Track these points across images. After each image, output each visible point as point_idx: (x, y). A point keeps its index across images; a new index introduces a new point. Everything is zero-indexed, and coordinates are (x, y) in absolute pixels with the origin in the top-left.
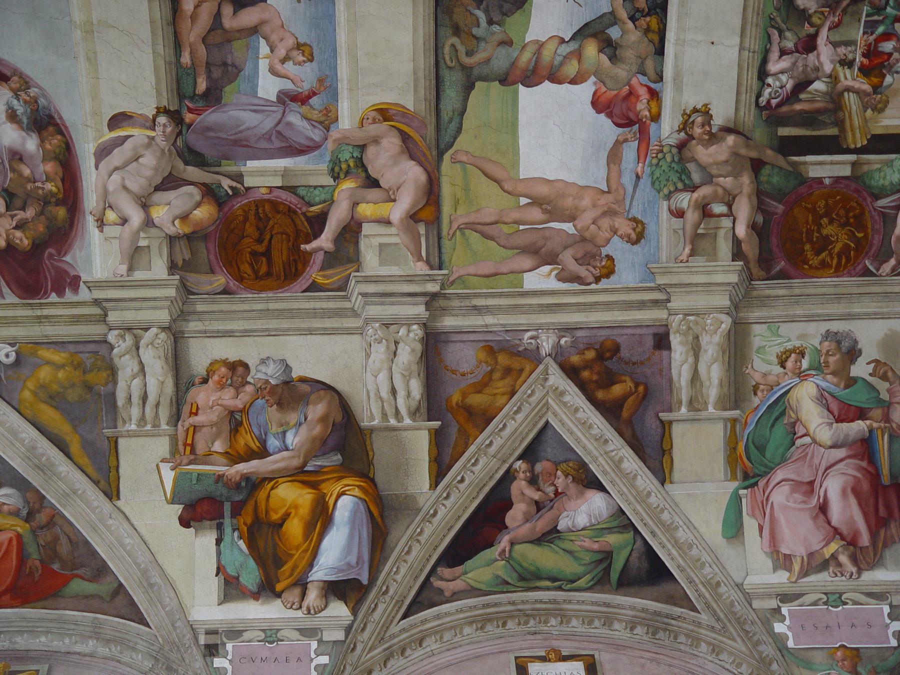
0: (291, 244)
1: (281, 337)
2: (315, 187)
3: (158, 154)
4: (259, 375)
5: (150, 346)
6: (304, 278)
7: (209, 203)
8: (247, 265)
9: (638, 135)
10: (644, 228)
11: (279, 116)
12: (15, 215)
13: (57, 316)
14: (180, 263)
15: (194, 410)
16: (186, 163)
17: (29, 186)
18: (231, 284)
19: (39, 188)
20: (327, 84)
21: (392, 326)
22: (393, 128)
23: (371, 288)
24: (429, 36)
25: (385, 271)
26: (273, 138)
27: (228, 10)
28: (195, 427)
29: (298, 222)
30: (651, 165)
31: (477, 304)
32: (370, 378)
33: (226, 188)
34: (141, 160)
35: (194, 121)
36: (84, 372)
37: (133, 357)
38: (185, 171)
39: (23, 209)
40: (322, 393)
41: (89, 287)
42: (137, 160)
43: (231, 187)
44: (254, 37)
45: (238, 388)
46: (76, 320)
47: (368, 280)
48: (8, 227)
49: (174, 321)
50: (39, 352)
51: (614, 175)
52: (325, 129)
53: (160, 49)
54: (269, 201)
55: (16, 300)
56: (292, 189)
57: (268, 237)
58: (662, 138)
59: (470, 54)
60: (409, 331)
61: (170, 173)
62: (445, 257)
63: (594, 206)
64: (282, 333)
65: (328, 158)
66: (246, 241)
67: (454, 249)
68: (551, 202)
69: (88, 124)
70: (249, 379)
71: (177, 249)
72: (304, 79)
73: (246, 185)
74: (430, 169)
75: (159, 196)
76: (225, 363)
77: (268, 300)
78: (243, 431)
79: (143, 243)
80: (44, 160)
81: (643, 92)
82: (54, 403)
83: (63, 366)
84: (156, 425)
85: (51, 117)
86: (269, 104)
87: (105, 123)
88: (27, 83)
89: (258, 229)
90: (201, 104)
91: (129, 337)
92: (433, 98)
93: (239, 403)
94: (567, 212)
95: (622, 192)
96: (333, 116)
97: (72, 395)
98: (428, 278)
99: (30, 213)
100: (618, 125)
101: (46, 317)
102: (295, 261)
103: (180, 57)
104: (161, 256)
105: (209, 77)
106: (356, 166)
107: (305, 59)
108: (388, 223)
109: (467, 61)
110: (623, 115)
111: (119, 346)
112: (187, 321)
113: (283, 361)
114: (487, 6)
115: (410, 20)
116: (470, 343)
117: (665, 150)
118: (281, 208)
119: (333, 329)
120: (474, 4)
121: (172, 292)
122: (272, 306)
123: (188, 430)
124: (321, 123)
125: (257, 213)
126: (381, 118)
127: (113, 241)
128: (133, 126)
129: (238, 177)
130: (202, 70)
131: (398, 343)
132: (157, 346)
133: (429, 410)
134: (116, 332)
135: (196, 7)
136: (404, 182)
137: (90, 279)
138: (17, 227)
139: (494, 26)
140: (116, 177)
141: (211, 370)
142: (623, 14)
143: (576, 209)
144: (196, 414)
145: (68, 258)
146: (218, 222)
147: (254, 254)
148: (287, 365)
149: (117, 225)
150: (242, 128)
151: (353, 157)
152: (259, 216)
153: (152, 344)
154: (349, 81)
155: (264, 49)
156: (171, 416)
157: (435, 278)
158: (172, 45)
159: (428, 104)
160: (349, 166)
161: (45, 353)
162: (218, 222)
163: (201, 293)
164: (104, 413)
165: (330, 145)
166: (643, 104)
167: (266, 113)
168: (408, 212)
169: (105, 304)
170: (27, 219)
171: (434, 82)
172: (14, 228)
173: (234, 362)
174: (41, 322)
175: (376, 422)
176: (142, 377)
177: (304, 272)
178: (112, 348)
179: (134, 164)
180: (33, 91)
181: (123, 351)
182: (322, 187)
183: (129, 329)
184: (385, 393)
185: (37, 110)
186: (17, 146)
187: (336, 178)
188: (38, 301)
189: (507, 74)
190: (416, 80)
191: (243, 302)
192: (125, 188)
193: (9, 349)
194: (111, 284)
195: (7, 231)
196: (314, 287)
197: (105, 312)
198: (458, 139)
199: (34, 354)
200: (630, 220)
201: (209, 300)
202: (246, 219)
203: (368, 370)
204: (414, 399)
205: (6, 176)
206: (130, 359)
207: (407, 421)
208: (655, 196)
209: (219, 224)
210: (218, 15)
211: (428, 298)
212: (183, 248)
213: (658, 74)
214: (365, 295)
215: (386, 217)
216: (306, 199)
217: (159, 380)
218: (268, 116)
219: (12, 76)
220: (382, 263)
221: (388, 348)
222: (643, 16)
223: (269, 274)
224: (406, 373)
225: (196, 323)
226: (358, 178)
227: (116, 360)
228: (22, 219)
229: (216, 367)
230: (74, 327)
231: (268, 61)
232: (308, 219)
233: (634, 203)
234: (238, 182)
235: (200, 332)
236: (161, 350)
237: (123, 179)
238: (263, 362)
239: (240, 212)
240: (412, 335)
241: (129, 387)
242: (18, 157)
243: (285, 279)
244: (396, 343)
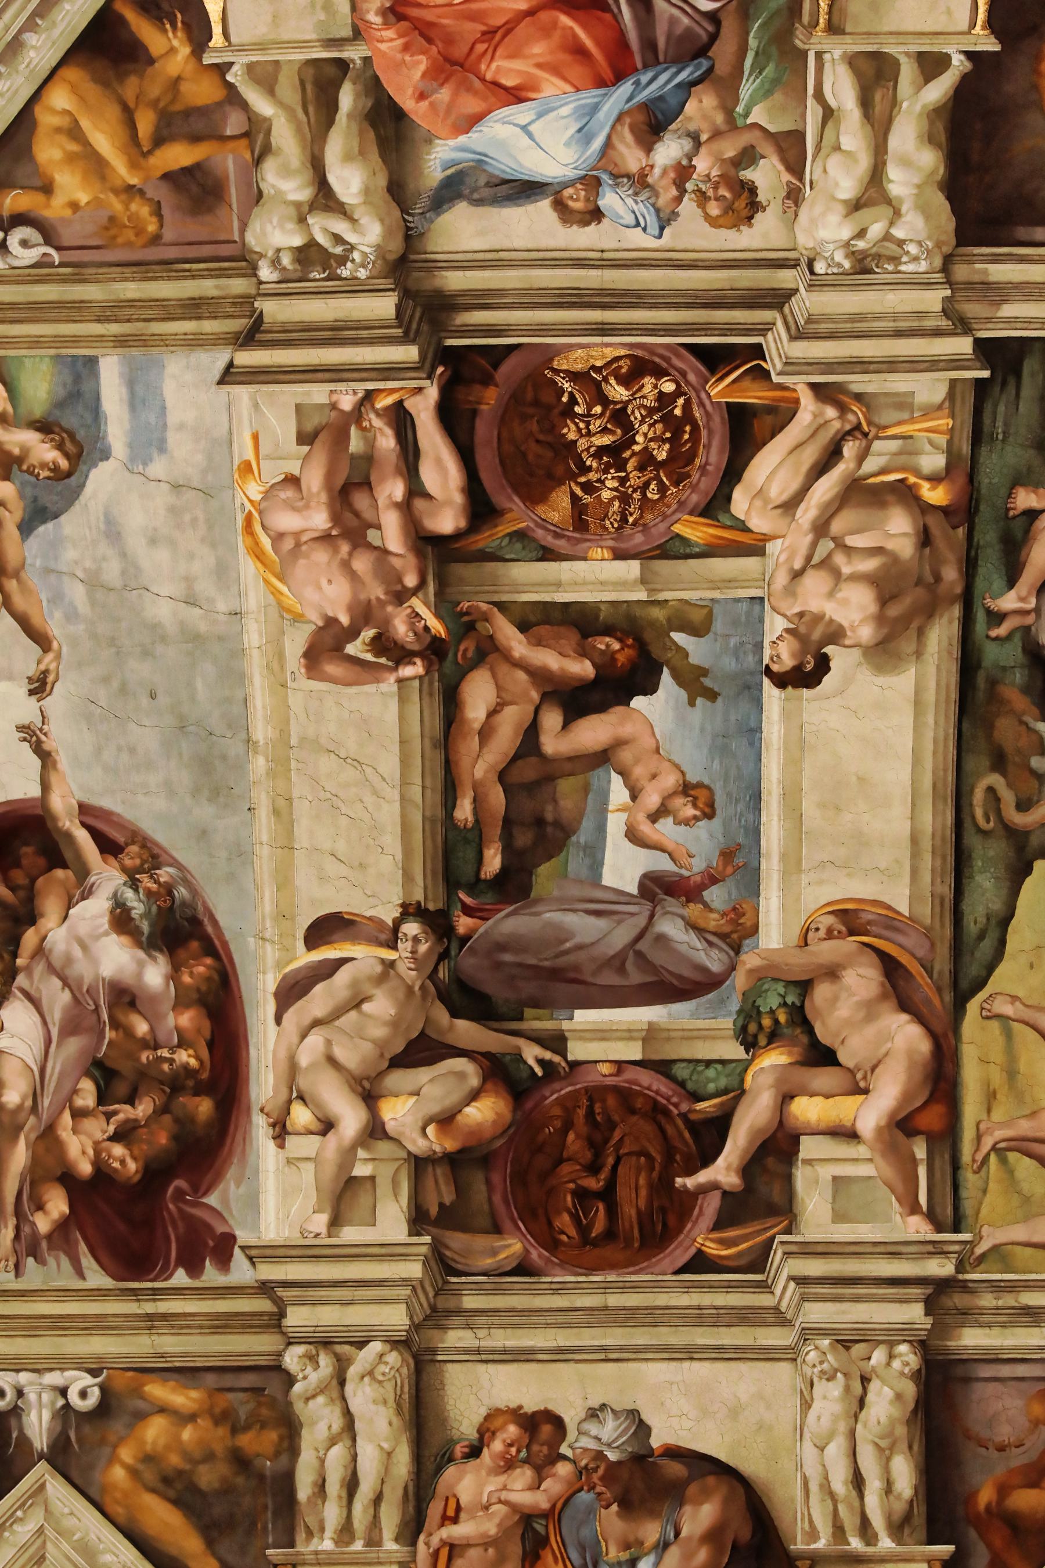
0: (655, 1174)
1: (631, 1365)
2: (708, 1063)
3: (401, 994)
4: (586, 1442)
5: (367, 1379)
6: (680, 1244)
7: (497, 1094)
8: (566, 1217)
11: (642, 921)
12: (115, 1113)
13: (185, 1315)
14: (434, 1210)
15: (451, 1512)
16: (455, 1014)
17: (145, 1056)
18: (534, 1255)
19: (162, 1059)
20: (739, 860)
21: (857, 1345)
22: (868, 950)
23: (814, 1267)
25: (844, 1233)
26: (630, 966)
27: (552, 719)
28: (452, 1547)
29: (670, 1130)
31: (1031, 1303)
32: (809, 1452)
33: (531, 1062)
34: (366, 1007)
35: (474, 930)
36: (235, 1431)
37: (332, 1400)
38: (451, 1027)
39: (131, 1101)
40: (711, 1480)
41: (251, 1259)
42: (358, 1005)
43: (541, 1062)
44: (600, 772)
45: (542, 1468)
46: (223, 1323)
47: (809, 1250)
48: (99, 1136)
49: (416, 1327)
50: (148, 1388)
52: (732, 948)
53: (416, 792)
54: (616, 1089)
55: (108, 1282)
56: (663, 1067)
57: (611, 1161)
59: (1023, 806)
60: (891, 1357)
61: (422, 1033)
62: (968, 1207)
64: (634, 1356)
65: (735, 1005)
66: (566, 1169)
67: (985, 1191)
69: (268, 935)
70: (564, 1449)
71: (430, 1183)
72: (693, 851)
73: (570, 1057)
74: (938, 1028)
75: (398, 1079)
76: (516, 1415)
77: (605, 1288)
78: (550, 1558)
79: (361, 1170)
80: (180, 1004)
82: (172, 1493)
83: (192, 1418)
84: (373, 1541)
85: (195, 922)
86: (622, 899)
87: (300, 934)
88: (154, 857)
89: (591, 1144)
90: (488, 898)
91: (326, 1362)
92: (947, 890)
93: (539, 1500)
96: (749, 924)
97: (207, 1477)
98: (930, 1248)
99: (143, 1109)
101: (164, 1317)
102: (663, 1210)
103: (454, 807)
104: (396, 1196)
105: (508, 849)
106: (792, 1022)
107: (698, 813)
108: (851, 1135)
109: (1020, 820)
111: (305, 1378)
112: (445, 1328)
113: (633, 1414)
115: (906, 742)
116: (1013, 1383)
118: (639, 1103)
119: (736, 1349)
120: (1036, 711)
121: (414, 1270)
122: (614, 1300)
123: (437, 1553)
124: (723, 936)
125: (590, 1113)
126: (844, 929)
127: (303, 1165)
128: (355, 939)
129: (557, 1042)
130: (494, 831)
131: (869, 1380)
132: (381, 1378)
133: (931, 1520)
134: (300, 1350)
135: (492, 714)
136: (886, 1054)
137: (253, 1242)
138: (115, 1138)
140: (315, 1040)
141: (488, 1430)
144: (455, 1520)
145: (212, 1200)
146: (512, 1131)
147: (582, 1195)
148: (641, 1421)
149: (312, 1133)
150: (568, 945)
151: (785, 1004)
152: (595, 1119)
153: (371, 1373)
154: (783, 857)
155: (618, 792)
156: (404, 1525)
157: (947, 1248)
158: (439, 786)
159: (937, 901)
160: (776, 1022)
161: (158, 1391)
162: (512, 1131)
163: (474, 1270)
164: (269, 1515)
165: (740, 980)
167: (615, 917)
168: (892, 1115)
169: (280, 1292)
170: (136, 1120)
171: (950, 860)
172: (111, 1139)
173: (535, 1414)
174: (150, 1328)
175: (821, 1544)
176: (348, 1443)
177: (680, 1231)
178: (290, 1380)
179: (353, 1014)
180: (165, 874)
181: (313, 1386)
182: (723, 1062)
183: (326, 1343)
184: (840, 1483)
185: (171, 908)
186: (128, 977)
187: (750, 1044)
188: (149, 1285)
190: (915, 854)
191: (558, 1289)
192: (332, 1061)
193: (87, 1380)
194: (294, 1252)
195: (96, 1144)
196: (700, 1263)
197: (279, 1307)
198: (998, 972)
199: (137, 1392)
201: (488, 1286)
202: (568, 1125)
203: (807, 1435)
204: (899, 1497)
205: (101, 1034)
206: (326, 1405)
207: (886, 1543)
209: (515, 1133)
210: (532, 732)
211: (929, 1290)
212: (441, 1181)
214: (801, 1281)
215: (849, 1124)
216: (690, 1086)
217: (381, 1448)
218: (619, 922)
219: (127, 845)
220: (839, 1217)
221: (847, 1389)
223: (610, 1235)
224: (883, 1444)
225: (460, 1333)
226: (794, 1046)
227: (299, 1407)
228: (127, 1121)
229: (498, 1422)
230: (216, 1337)
231: (624, 816)
232: (691, 1125)
234: (555, 1051)
235: (467, 1351)
236: (389, 1386)
237: (329, 1043)
238: (594, 1414)
239: (557, 1111)
240: (896, 1364)
241: (322, 1461)
242: (126, 999)
243: (643, 1245)
244: (865, 1380)
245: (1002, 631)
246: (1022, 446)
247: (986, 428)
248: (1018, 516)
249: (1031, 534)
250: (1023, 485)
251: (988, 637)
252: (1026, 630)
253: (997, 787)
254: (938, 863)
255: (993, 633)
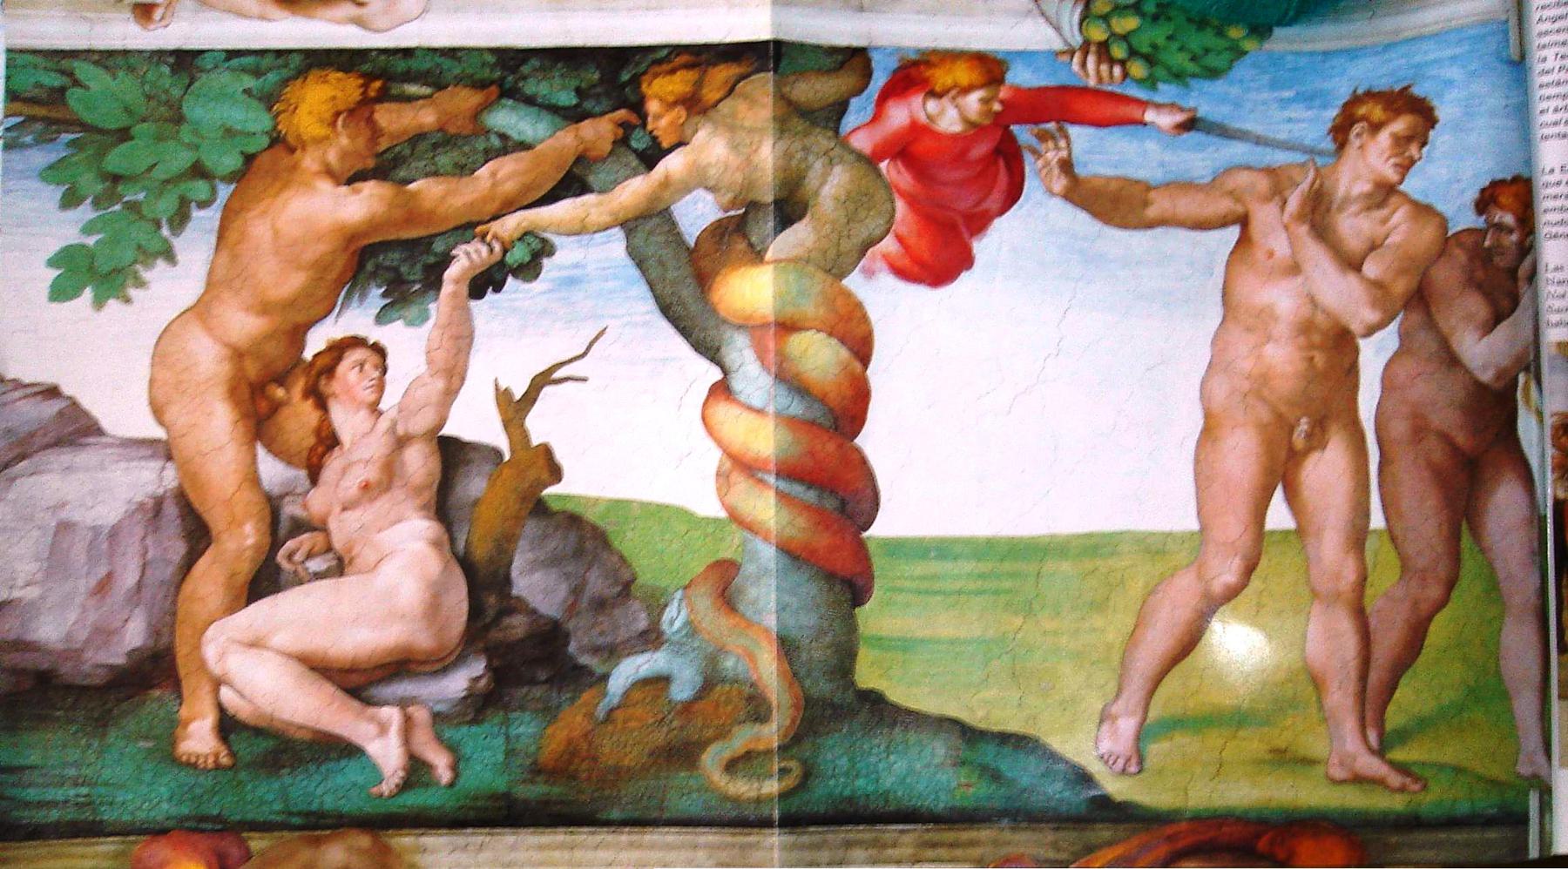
9: (1051, 126)
10: (1370, 95)
24: (695, 847)
30: (1150, 82)
51: (1187, 205)
58: (1058, 45)
63: (1294, 269)
68: (1280, 417)
81: (899, 116)
94: (1320, 359)
95: (1243, 178)
100: (1013, 195)
110: (980, 175)
114: (596, 650)
117: (1098, 33)
139: (665, 626)
142: (634, 190)
143: (1306, 328)
166: (942, 112)
189: (830, 576)
200: (1342, 145)
208: (1254, 65)
213: (842, 65)
222: (644, 125)
233: (1282, 136)
245: (440, 762)
246: (100, 753)
247: (70, 814)
248: (229, 748)
249: (264, 724)
250: (173, 742)
251: (451, 785)
252: (438, 718)
253: (727, 754)
254: (858, 853)
255: (444, 775)
